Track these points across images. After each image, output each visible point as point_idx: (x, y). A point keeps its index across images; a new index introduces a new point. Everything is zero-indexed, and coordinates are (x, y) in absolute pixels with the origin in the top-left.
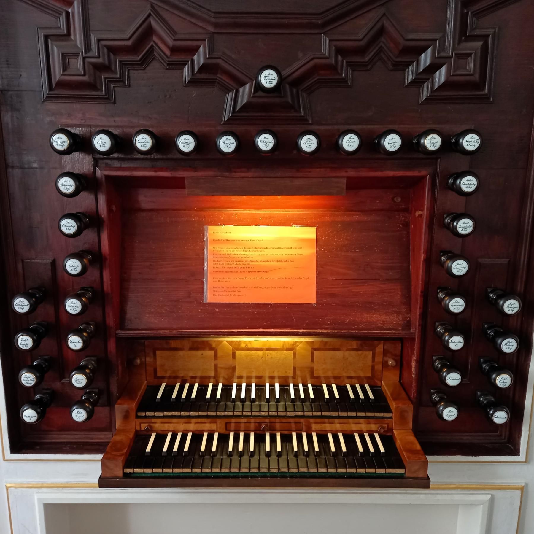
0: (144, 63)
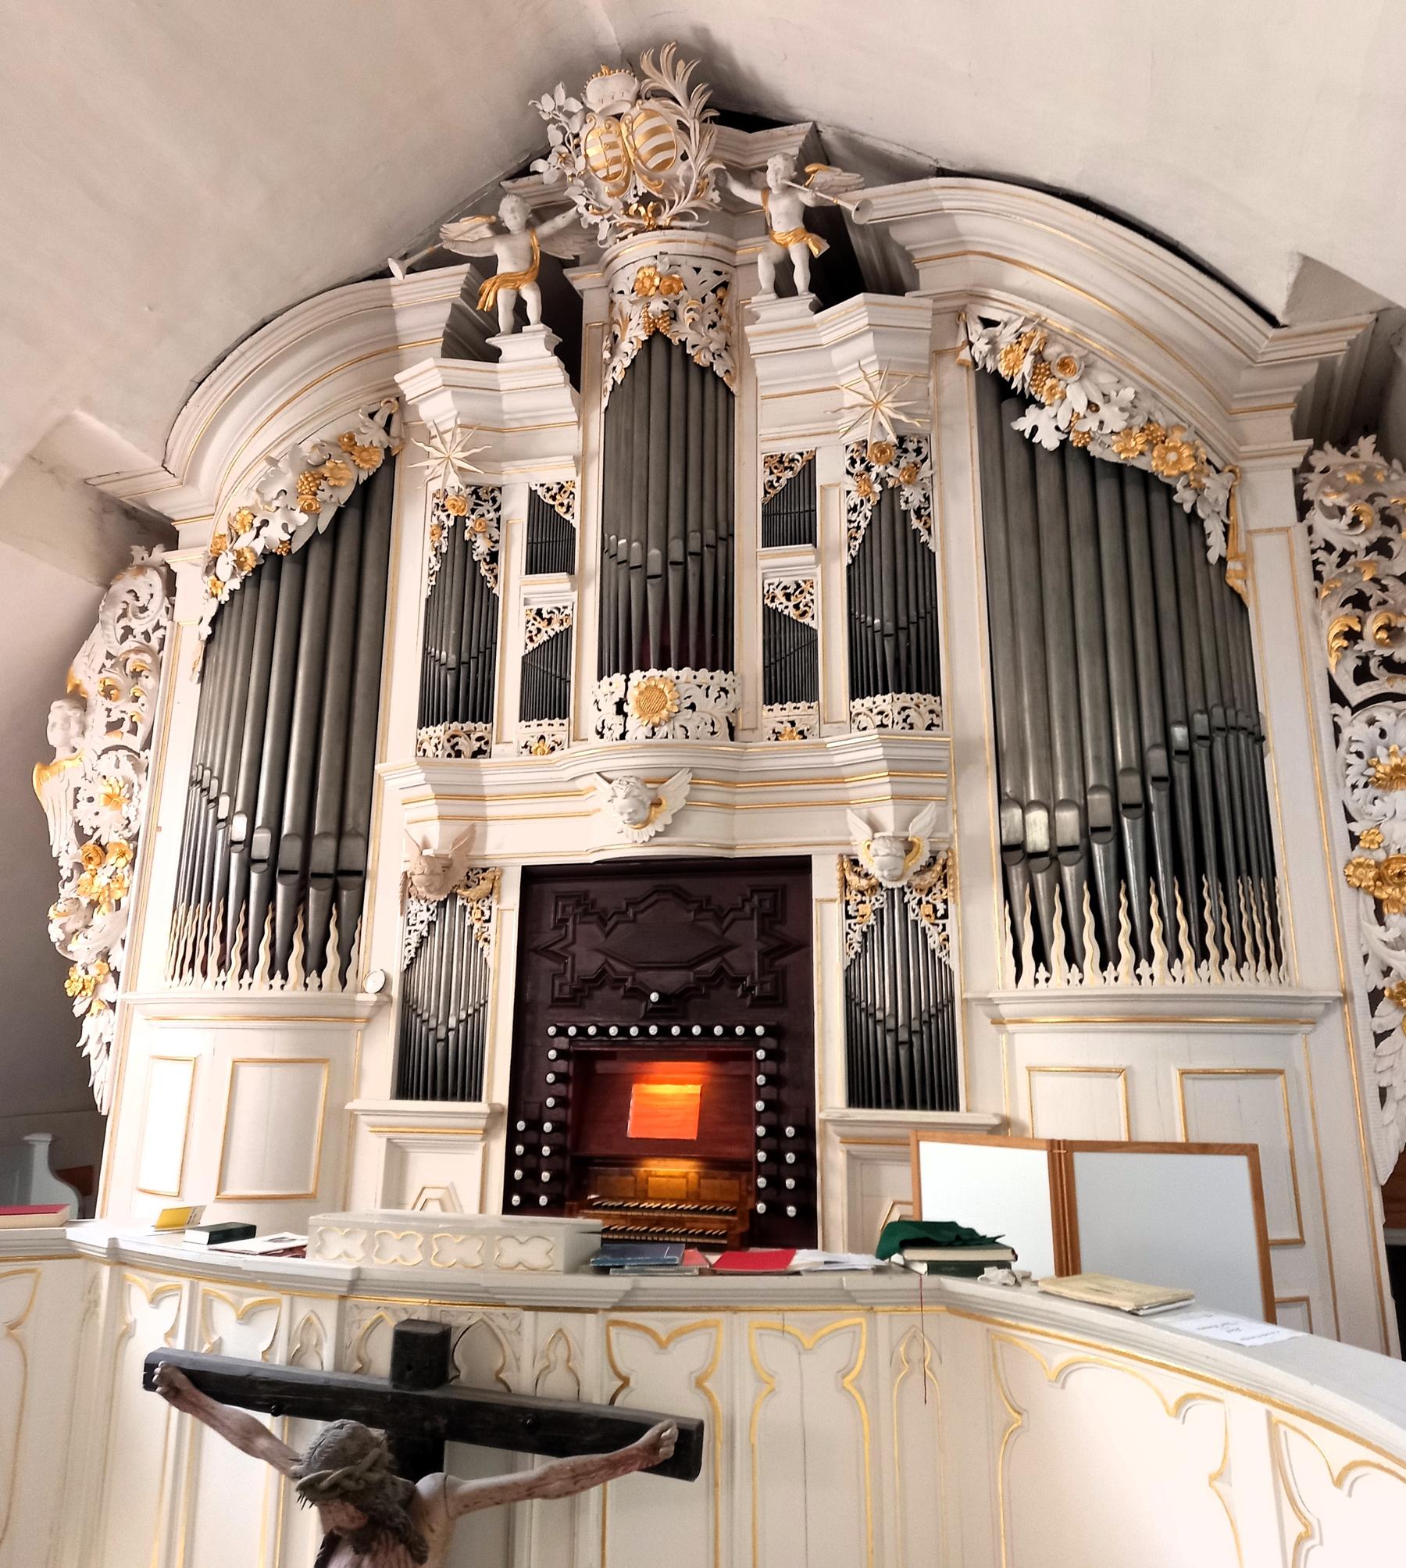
0: (600, 987)
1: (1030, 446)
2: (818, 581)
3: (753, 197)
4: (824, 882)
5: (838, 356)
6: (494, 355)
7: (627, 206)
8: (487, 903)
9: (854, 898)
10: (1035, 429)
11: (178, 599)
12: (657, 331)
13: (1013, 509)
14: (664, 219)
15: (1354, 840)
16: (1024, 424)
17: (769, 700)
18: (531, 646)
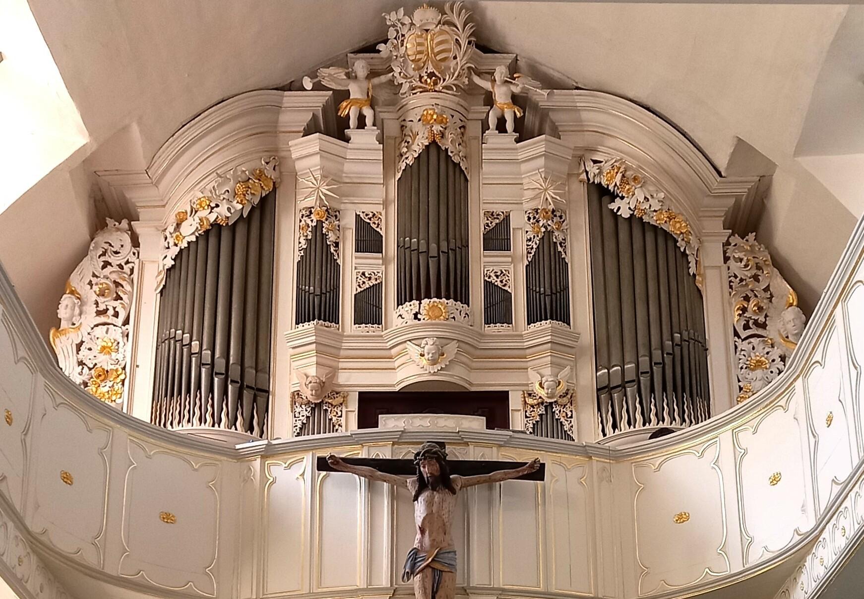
1: (615, 216)
2: (512, 271)
3: (486, 85)
4: (515, 402)
5: (524, 167)
6: (347, 140)
7: (421, 77)
8: (339, 409)
9: (529, 409)
10: (619, 208)
11: (141, 249)
12: (434, 142)
13: (606, 243)
14: (439, 87)
15: (741, 389)
16: (613, 206)
17: (487, 323)
18: (359, 290)
